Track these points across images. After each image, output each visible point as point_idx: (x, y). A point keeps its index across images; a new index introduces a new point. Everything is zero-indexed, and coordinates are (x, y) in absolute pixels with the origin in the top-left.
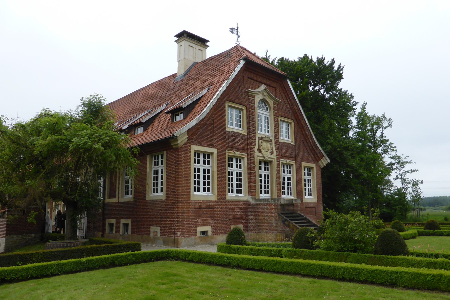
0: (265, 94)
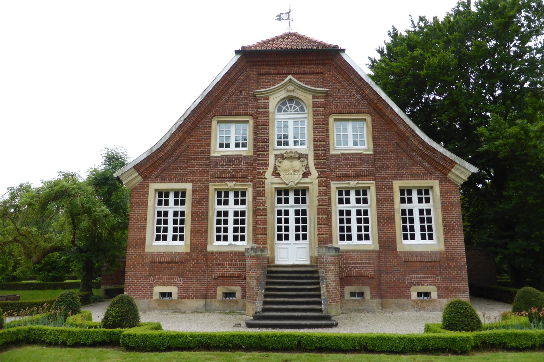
0: (291, 88)
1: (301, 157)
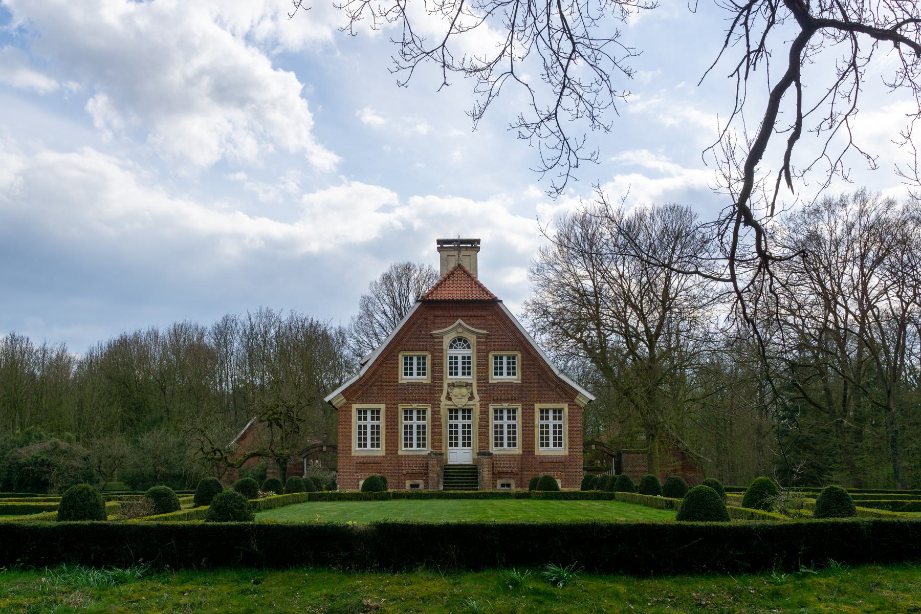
0: (460, 330)
1: (468, 385)
